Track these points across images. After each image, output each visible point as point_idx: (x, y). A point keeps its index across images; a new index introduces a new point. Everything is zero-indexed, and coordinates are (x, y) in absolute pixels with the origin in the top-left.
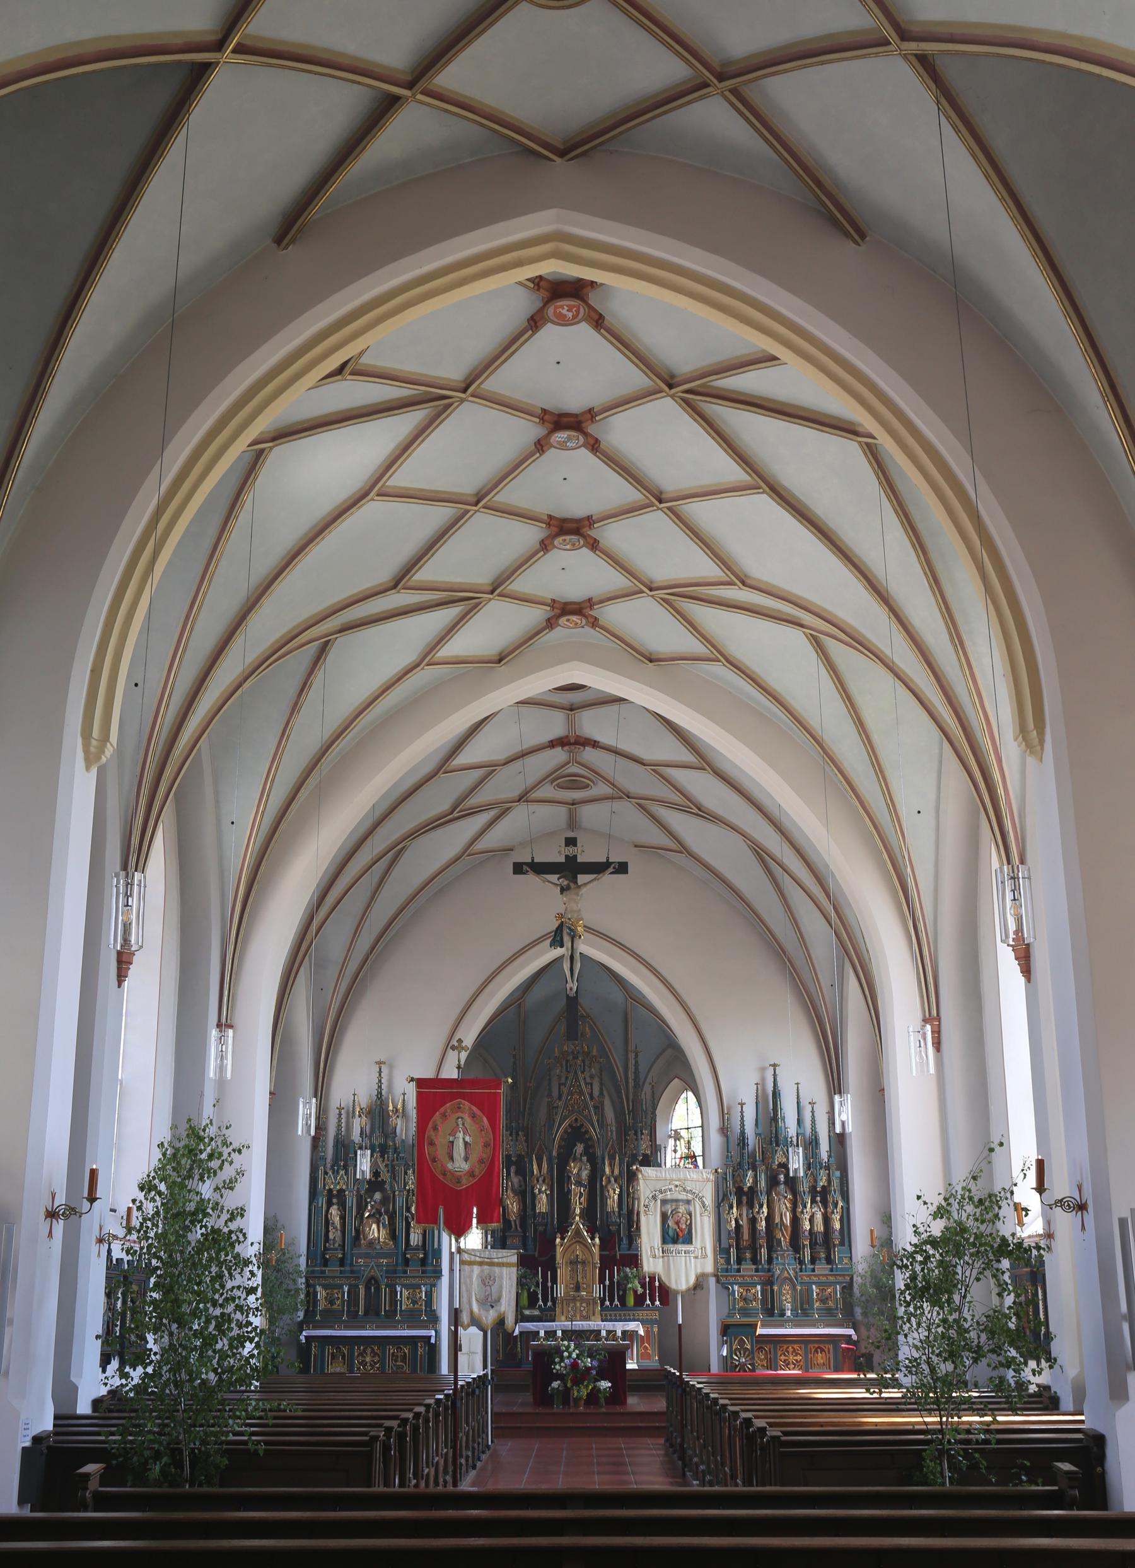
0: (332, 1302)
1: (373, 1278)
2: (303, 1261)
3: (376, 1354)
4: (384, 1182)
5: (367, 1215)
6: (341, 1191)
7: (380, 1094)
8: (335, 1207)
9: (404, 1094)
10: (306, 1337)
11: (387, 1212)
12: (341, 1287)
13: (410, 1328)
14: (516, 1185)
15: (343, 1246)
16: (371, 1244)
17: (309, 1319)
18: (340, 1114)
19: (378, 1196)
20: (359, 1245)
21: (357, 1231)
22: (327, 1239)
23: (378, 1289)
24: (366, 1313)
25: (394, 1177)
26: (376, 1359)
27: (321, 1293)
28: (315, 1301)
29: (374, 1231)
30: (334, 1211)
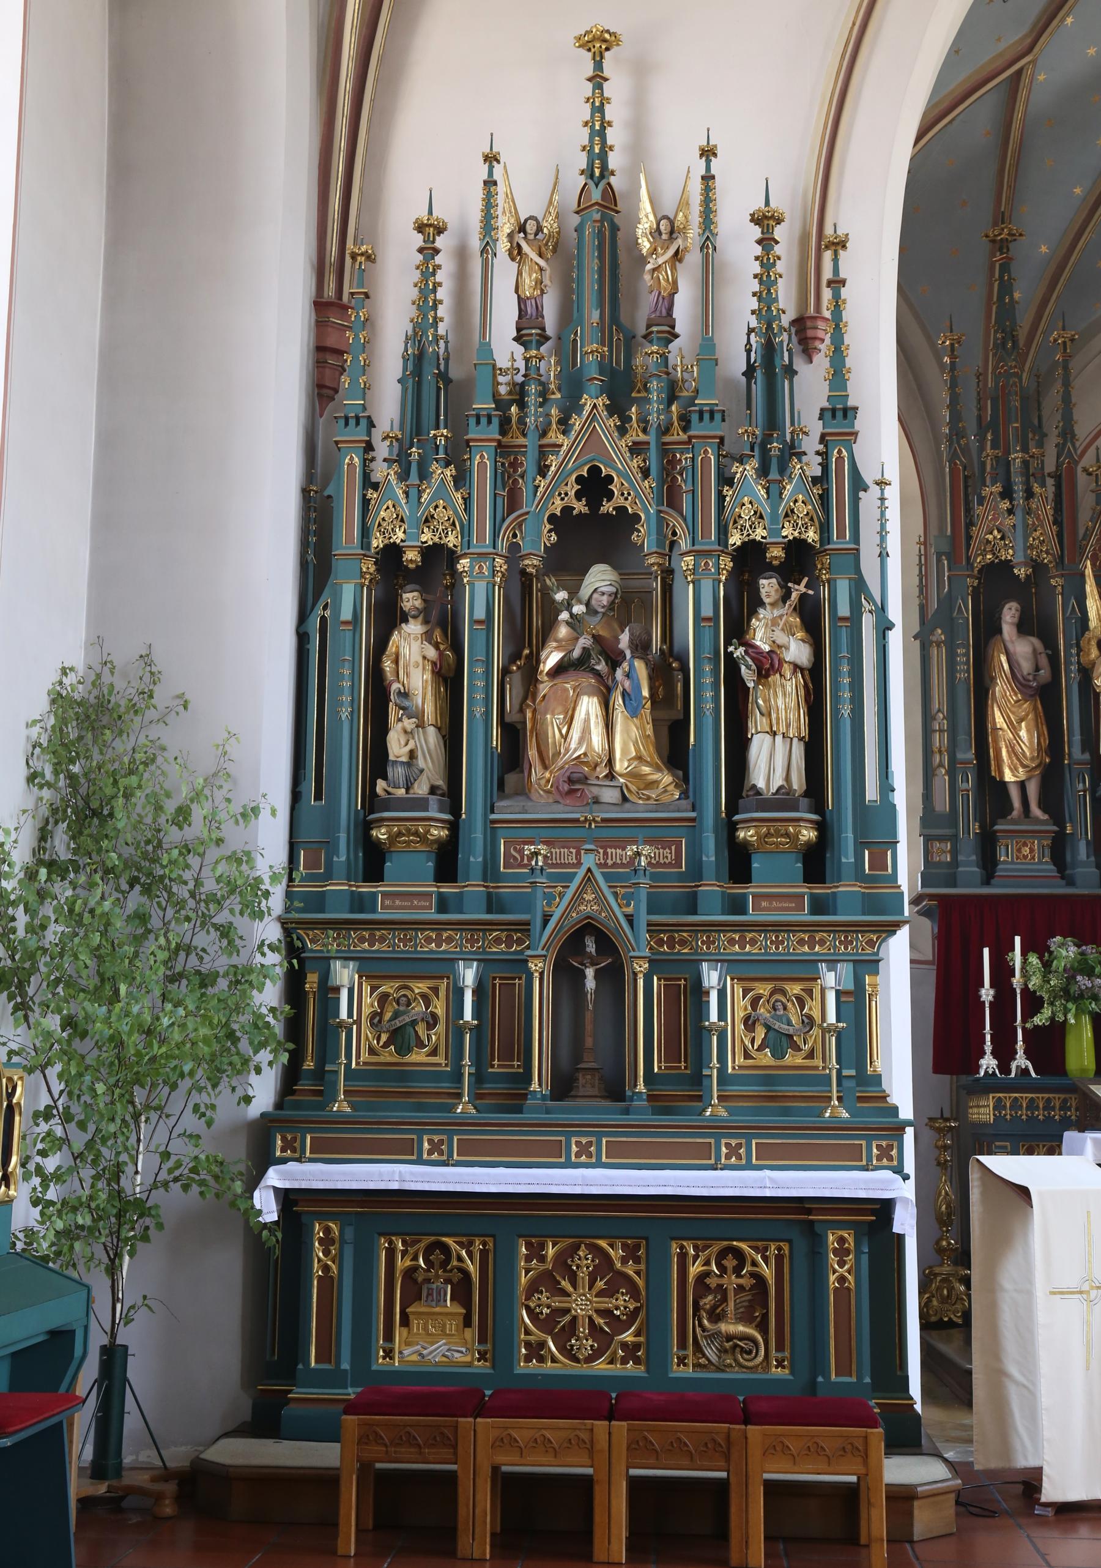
0: (401, 1038)
1: (589, 927)
2: (270, 842)
3: (618, 1282)
4: (626, 520)
5: (552, 659)
6: (438, 558)
7: (597, 169)
8: (414, 628)
9: (708, 153)
10: (287, 1198)
11: (641, 647)
12: (441, 969)
13: (775, 1156)
14: (1026, 666)
15: (451, 793)
16: (575, 782)
17: (300, 1115)
18: (429, 251)
19: (600, 579)
20: (523, 791)
21: (514, 736)
22: (377, 760)
23: (614, 976)
24: (563, 1087)
25: (670, 497)
26: (622, 1303)
27: (351, 989)
28: (329, 1029)
29: (592, 729)
30: (412, 650)
